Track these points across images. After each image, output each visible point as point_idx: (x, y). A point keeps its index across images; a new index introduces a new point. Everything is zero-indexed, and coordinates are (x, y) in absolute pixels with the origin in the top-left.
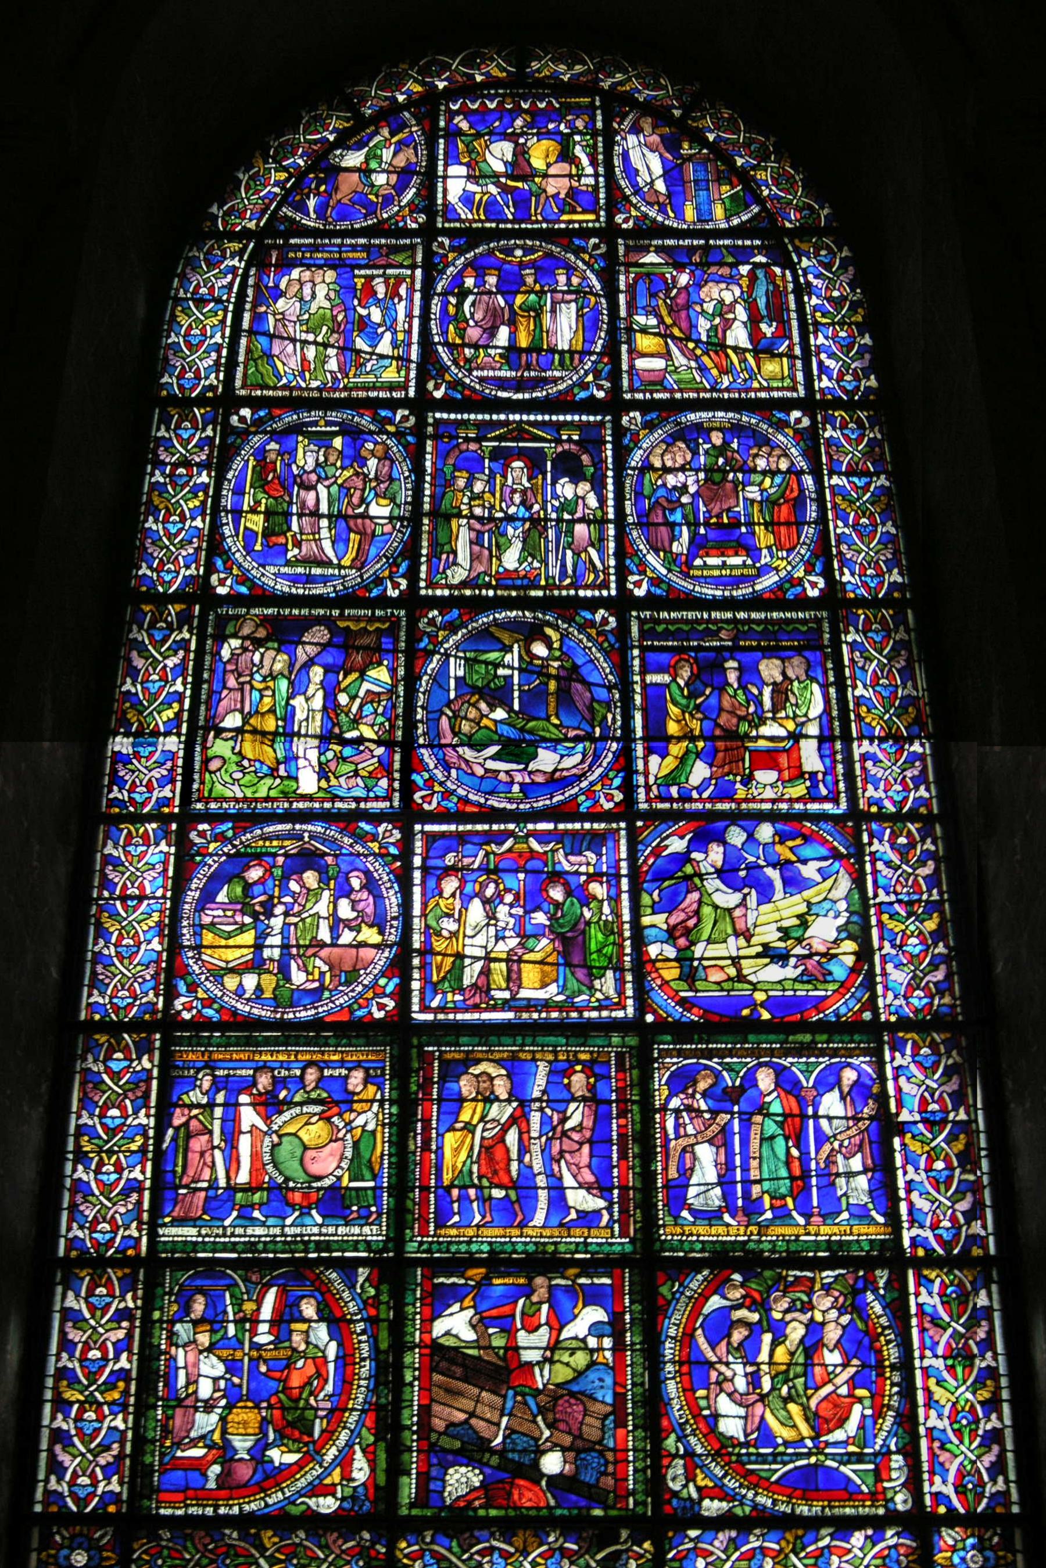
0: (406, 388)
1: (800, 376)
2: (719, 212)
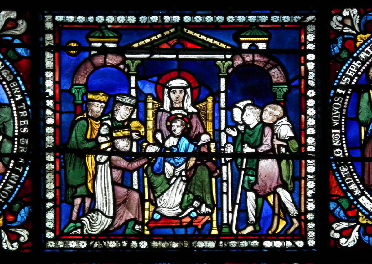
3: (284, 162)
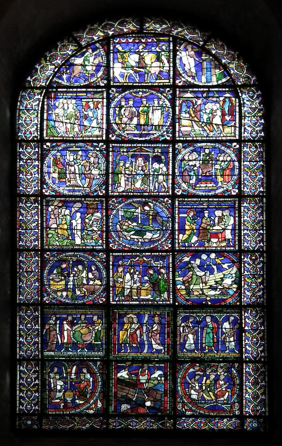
0: (102, 137)
1: (237, 133)
2: (214, 79)
3: (164, 176)
